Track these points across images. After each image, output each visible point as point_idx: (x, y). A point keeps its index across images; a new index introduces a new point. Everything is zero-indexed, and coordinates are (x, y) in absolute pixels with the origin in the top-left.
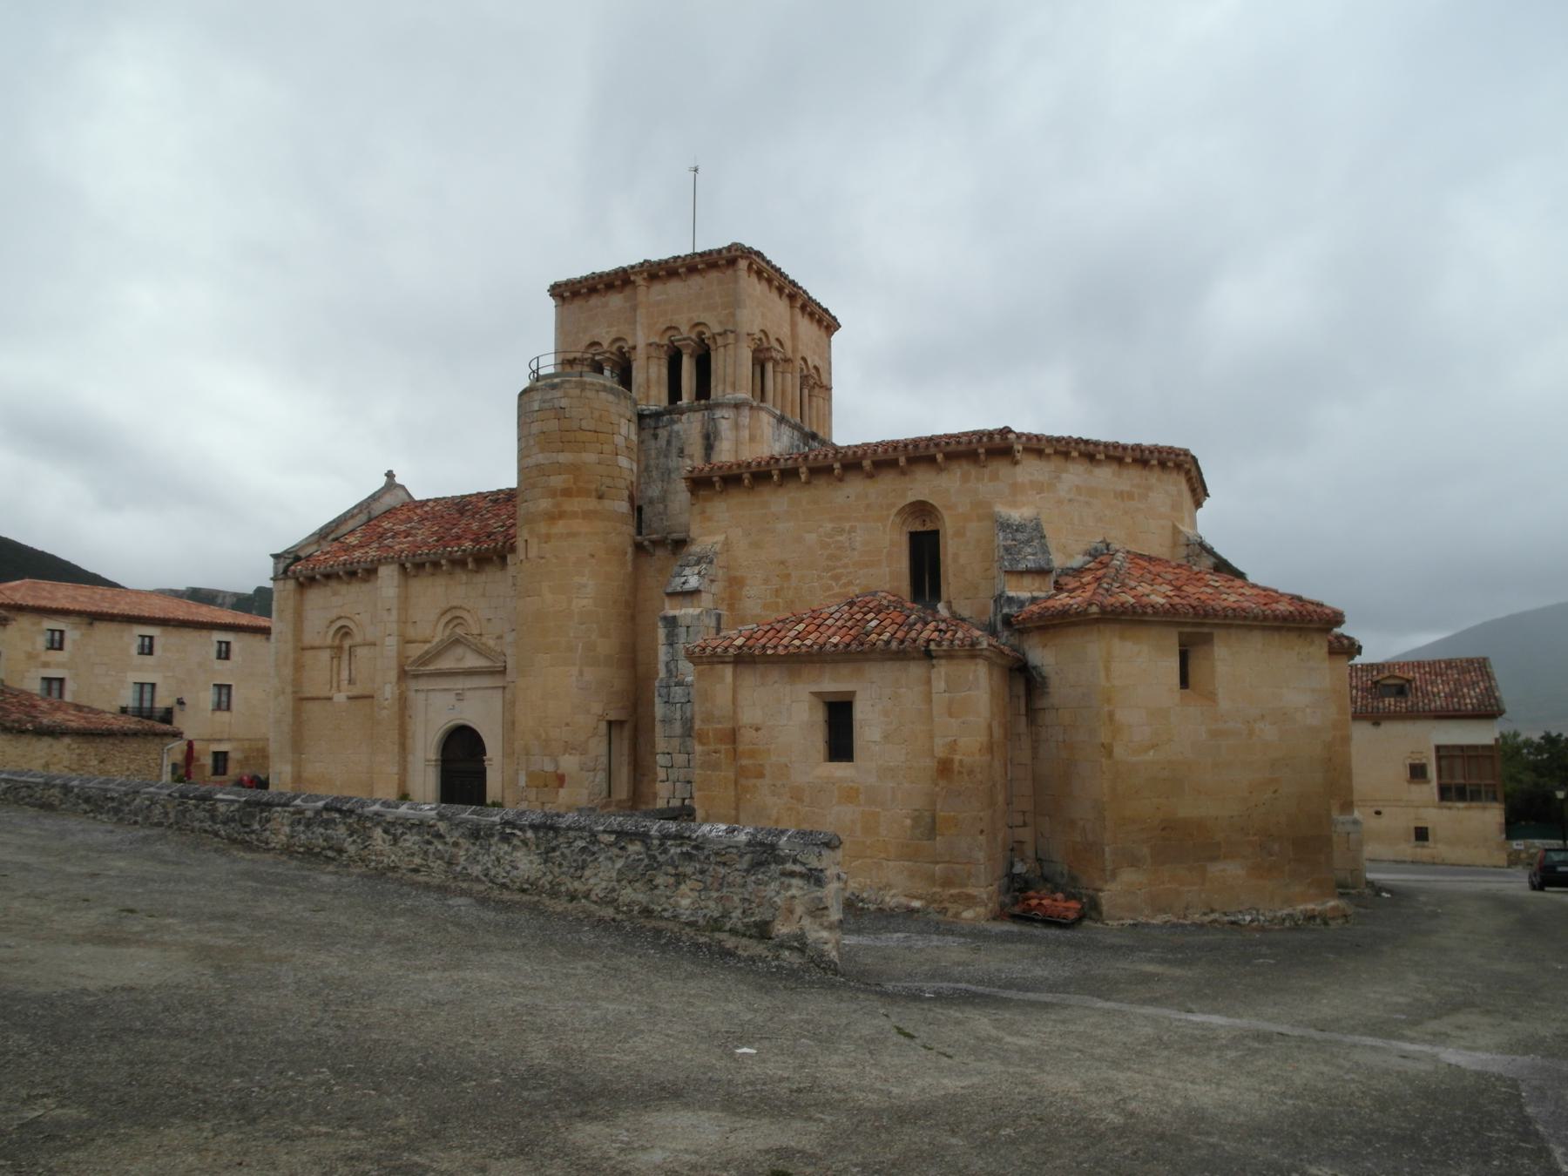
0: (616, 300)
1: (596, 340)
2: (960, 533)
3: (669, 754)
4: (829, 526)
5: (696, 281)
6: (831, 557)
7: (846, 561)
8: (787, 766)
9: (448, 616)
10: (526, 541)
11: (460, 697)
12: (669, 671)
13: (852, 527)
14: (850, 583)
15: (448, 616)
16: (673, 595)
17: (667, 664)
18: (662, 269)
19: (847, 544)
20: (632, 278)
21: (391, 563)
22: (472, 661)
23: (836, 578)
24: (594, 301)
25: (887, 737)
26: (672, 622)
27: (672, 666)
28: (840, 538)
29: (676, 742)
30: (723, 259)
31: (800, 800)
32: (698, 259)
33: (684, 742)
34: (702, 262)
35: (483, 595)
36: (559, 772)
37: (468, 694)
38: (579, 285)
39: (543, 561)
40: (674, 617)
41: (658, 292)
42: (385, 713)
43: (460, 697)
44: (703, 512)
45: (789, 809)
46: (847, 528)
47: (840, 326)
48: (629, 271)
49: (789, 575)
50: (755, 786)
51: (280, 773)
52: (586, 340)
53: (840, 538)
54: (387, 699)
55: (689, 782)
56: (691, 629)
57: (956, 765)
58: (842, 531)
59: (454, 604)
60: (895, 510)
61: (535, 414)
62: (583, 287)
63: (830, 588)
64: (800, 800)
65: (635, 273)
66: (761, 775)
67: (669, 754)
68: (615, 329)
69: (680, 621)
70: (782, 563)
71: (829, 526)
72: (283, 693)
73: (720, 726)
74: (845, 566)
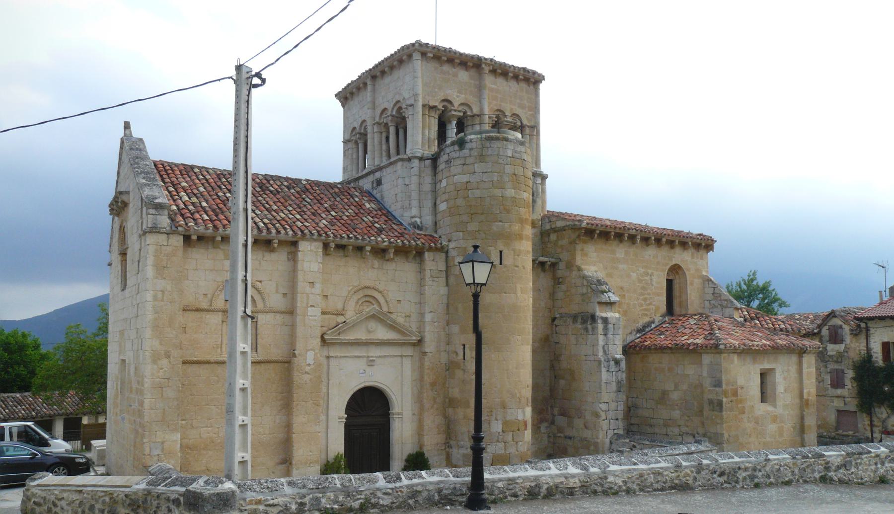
0: (463, 75)
1: (449, 98)
2: (692, 284)
3: (607, 403)
4: (642, 270)
5: (513, 84)
6: (643, 288)
7: (649, 291)
8: (753, 406)
9: (361, 294)
10: (501, 252)
11: (371, 363)
12: (604, 351)
13: (652, 273)
14: (650, 304)
15: (361, 294)
16: (600, 303)
17: (603, 347)
18: (500, 69)
19: (649, 282)
20: (483, 66)
21: (315, 240)
22: (383, 333)
23: (645, 300)
24: (446, 68)
25: (785, 390)
26: (605, 320)
27: (606, 348)
28: (646, 278)
29: (613, 395)
30: (533, 78)
31: (758, 423)
32: (522, 72)
33: (618, 395)
34: (523, 75)
35: (393, 280)
36: (525, 420)
37: (379, 361)
38: (444, 53)
39: (516, 269)
40: (606, 318)
41: (500, 84)
42: (306, 377)
43: (371, 363)
44: (582, 250)
45: (754, 428)
46: (650, 273)
47: (336, 96)
48: (483, 61)
49: (624, 295)
50: (742, 418)
51: (163, 443)
52: (441, 96)
53: (646, 278)
54: (309, 365)
55: (617, 419)
56: (616, 326)
57: (810, 403)
58: (647, 274)
59: (368, 284)
60: (668, 267)
61: (509, 159)
62: (445, 56)
63: (641, 305)
64: (758, 423)
65: (486, 64)
66: (744, 413)
67: (607, 403)
68: (463, 96)
69: (610, 320)
70: (622, 288)
71: (642, 270)
72: (168, 357)
73: (733, 387)
74: (649, 294)
